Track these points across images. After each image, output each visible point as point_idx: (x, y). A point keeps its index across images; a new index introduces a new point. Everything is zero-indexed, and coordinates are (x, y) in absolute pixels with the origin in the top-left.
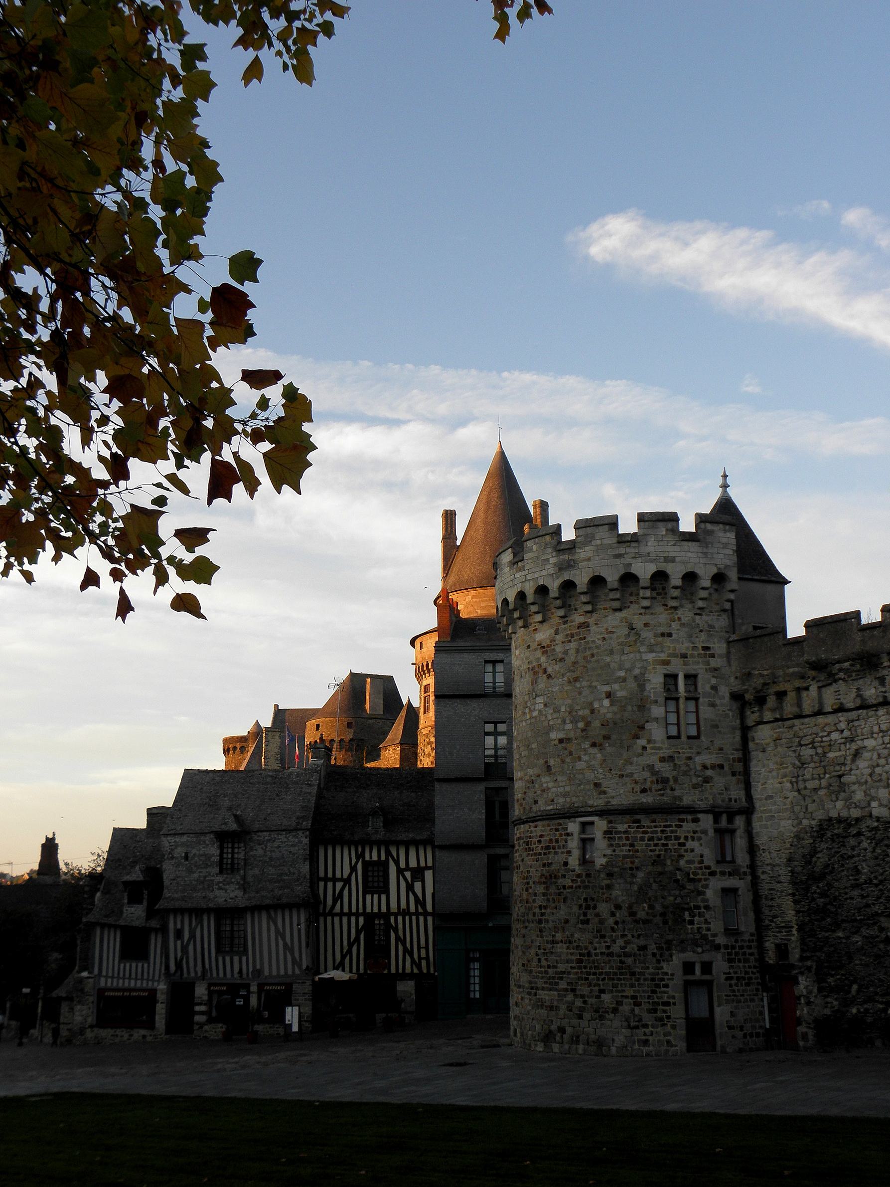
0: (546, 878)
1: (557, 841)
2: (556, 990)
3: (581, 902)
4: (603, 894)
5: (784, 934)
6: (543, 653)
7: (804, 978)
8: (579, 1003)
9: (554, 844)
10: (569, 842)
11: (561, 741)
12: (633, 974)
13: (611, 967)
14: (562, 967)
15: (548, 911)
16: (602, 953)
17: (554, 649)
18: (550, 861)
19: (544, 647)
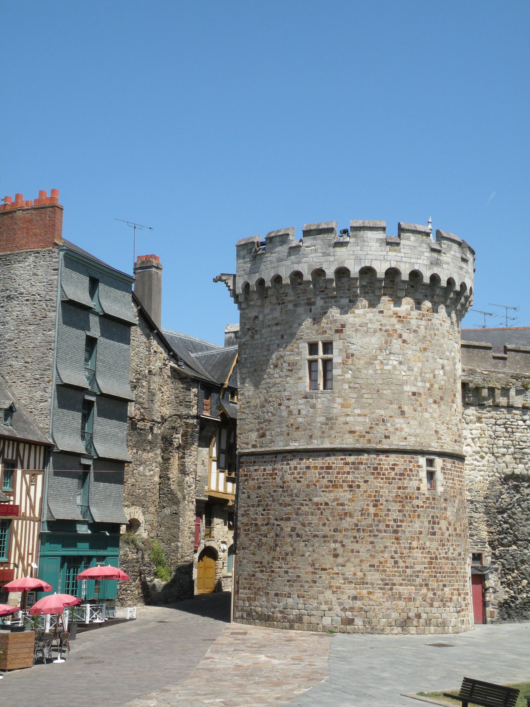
0: (402, 498)
1: (411, 470)
2: (414, 586)
3: (430, 519)
4: (443, 513)
5: (479, 546)
6: (399, 321)
7: (493, 576)
8: (430, 594)
9: (409, 472)
10: (420, 472)
11: (414, 394)
12: (457, 573)
13: (448, 568)
14: (418, 568)
15: (404, 524)
16: (444, 557)
17: (409, 321)
18: (405, 486)
19: (400, 317)
